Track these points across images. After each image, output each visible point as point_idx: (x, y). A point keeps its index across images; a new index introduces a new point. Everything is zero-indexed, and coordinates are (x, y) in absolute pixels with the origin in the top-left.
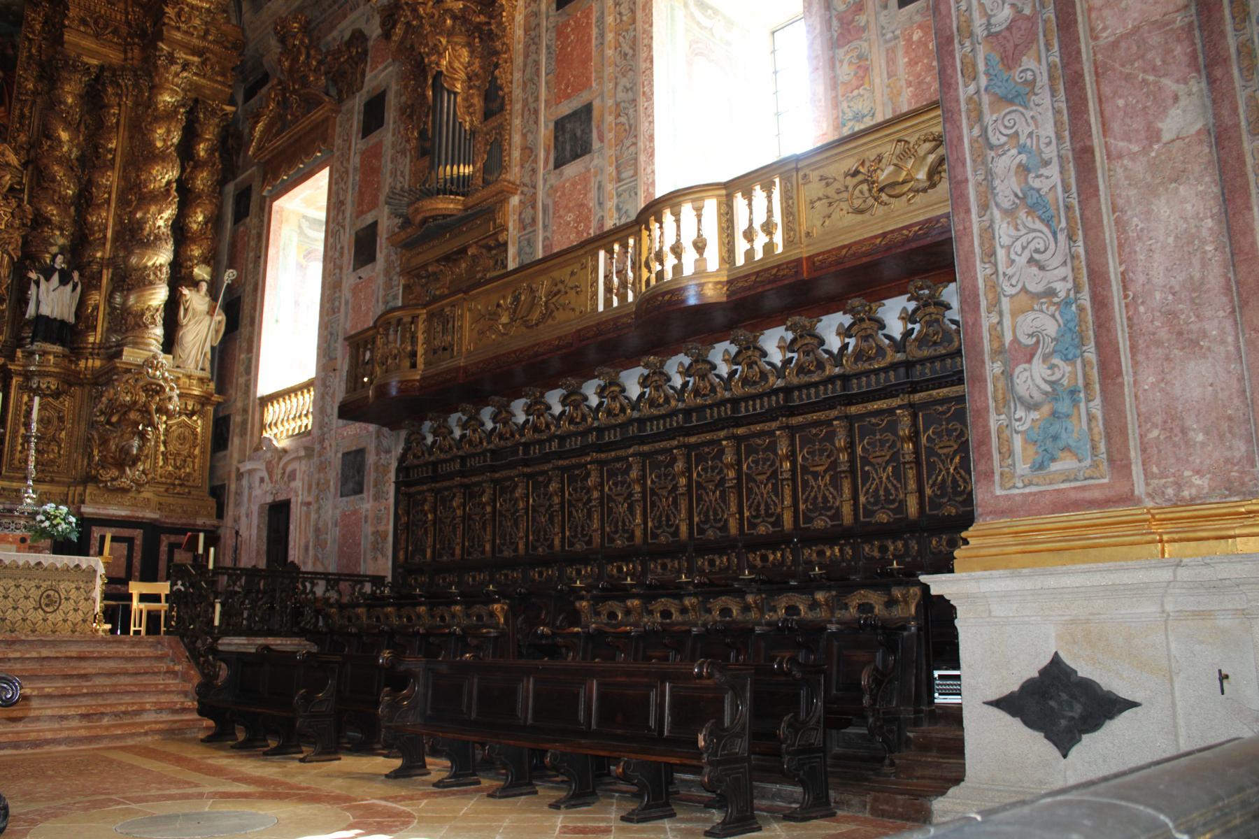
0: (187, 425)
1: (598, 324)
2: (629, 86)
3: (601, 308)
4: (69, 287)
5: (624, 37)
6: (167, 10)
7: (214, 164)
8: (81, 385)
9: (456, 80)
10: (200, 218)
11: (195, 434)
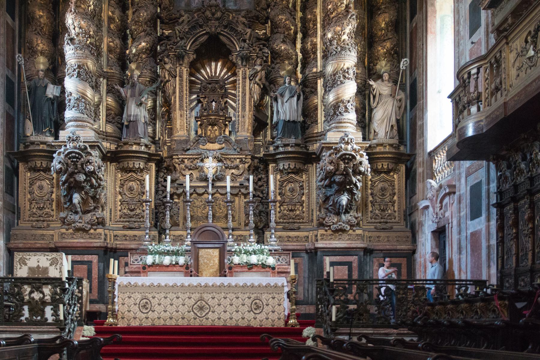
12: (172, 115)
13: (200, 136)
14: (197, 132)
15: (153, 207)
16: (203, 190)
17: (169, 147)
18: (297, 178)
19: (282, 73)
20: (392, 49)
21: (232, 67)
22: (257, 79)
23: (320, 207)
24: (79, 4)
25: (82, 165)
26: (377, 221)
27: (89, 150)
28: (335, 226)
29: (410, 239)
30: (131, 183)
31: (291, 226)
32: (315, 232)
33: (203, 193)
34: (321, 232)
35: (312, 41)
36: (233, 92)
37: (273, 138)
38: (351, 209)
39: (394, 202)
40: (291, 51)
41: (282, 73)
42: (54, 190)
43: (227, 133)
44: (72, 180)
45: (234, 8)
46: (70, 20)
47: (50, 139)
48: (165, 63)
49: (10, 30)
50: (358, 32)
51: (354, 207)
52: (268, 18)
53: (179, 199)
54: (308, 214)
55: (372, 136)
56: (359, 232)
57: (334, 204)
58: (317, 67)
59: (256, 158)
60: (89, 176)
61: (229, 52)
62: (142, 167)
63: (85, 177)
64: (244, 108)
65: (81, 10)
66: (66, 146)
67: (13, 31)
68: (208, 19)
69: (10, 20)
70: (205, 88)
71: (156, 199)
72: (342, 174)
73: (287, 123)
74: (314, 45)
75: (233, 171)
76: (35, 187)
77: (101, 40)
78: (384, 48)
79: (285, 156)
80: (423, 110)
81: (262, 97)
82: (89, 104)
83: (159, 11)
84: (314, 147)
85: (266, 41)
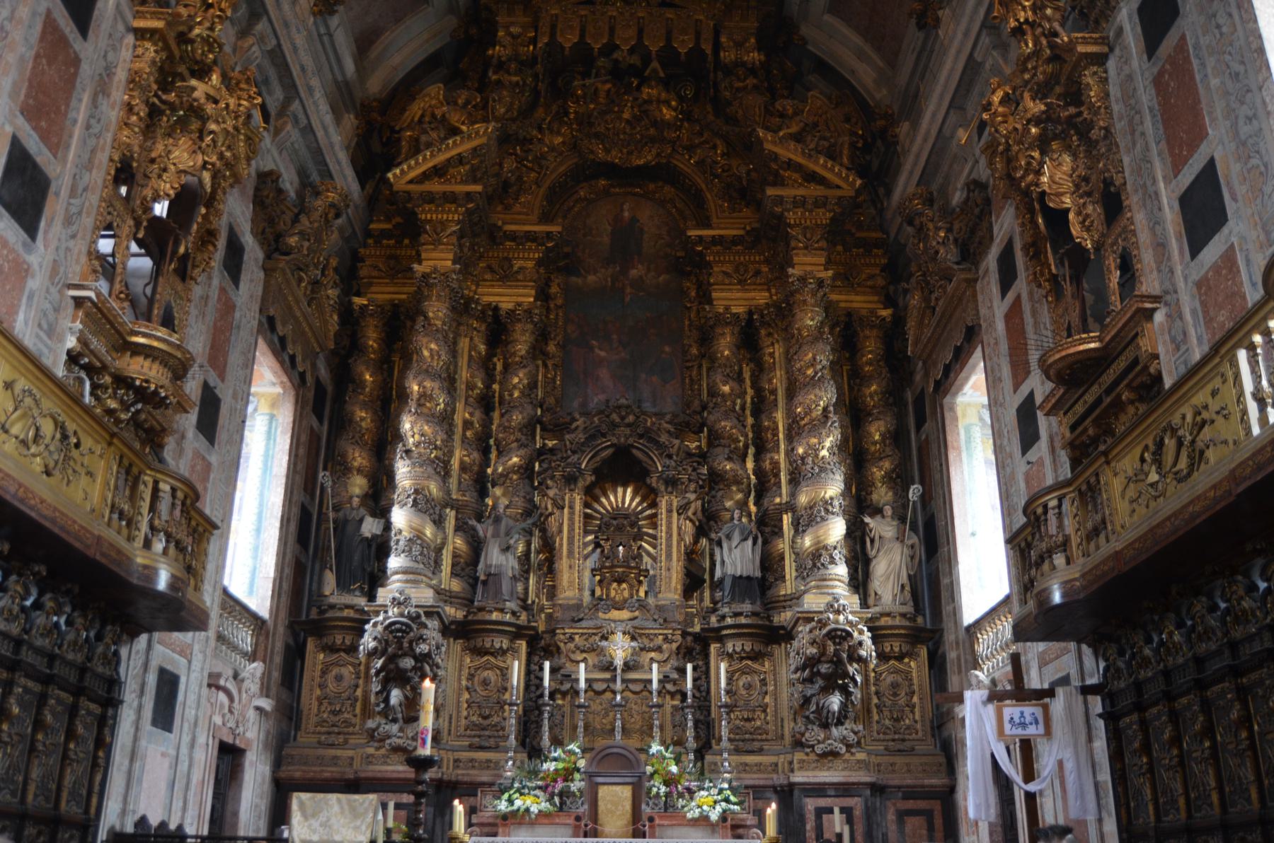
0: (897, 671)
1: (1254, 455)
2: (1250, 113)
3: (1256, 430)
5: (1230, 54)
9: (1063, 194)
12: (556, 565)
13: (600, 599)
14: (593, 593)
15: (521, 712)
16: (605, 686)
17: (550, 616)
18: (756, 666)
19: (728, 504)
20: (893, 470)
21: (650, 496)
22: (690, 513)
23: (795, 713)
24: (422, 401)
25: (411, 643)
26: (887, 737)
27: (423, 619)
28: (821, 746)
29: (944, 768)
30: (486, 673)
31: (748, 746)
32: (789, 757)
33: (605, 691)
34: (799, 756)
35: (772, 459)
36: (650, 531)
37: (714, 602)
38: (846, 717)
39: (914, 706)
40: (740, 472)
41: (728, 504)
42: (361, 682)
43: (642, 594)
44: (392, 666)
45: (654, 410)
46: (406, 425)
47: (361, 601)
48: (548, 488)
49: (314, 437)
50: (842, 447)
51: (851, 715)
52: (703, 425)
53: (563, 698)
54: (776, 725)
55: (871, 601)
56: (861, 756)
57: (819, 710)
58: (780, 495)
59: (690, 634)
60: (421, 662)
61: (645, 473)
62: (505, 647)
63: (413, 663)
64: (669, 556)
65: (425, 410)
66: (386, 612)
67: (319, 439)
68: (614, 425)
69: (315, 423)
70: (608, 525)
71: (525, 700)
72: (831, 661)
73: (737, 580)
74: (776, 465)
75: (653, 654)
76: (330, 677)
77: (451, 453)
78: (881, 469)
79: (732, 631)
80: (951, 560)
81: (696, 541)
82: (428, 547)
83: (539, 412)
84: (784, 617)
85: (703, 456)
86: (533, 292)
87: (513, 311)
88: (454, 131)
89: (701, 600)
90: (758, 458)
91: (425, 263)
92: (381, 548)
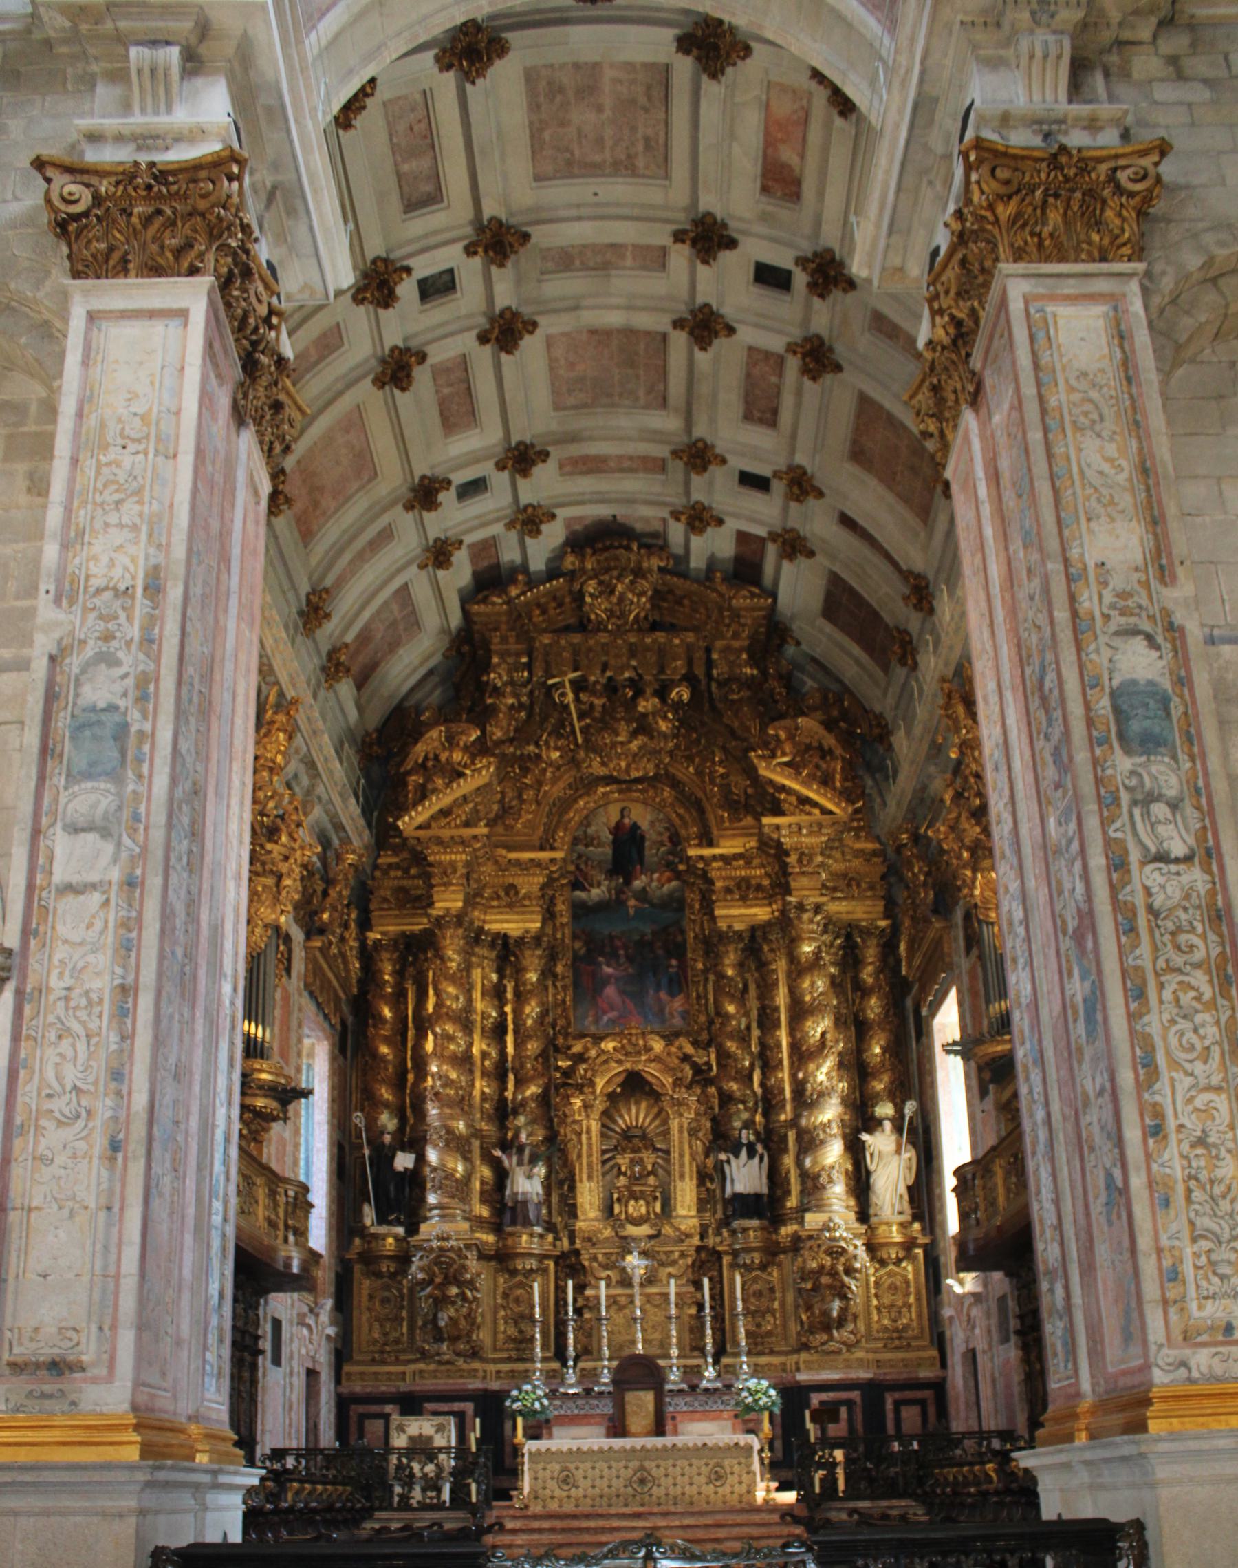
4: (756, 1160)
6: (788, 860)
7: (880, 988)
8: (784, 1252)
10: (877, 1050)
11: (907, 1282)
39: (910, 1306)
75: (670, 1270)
77: (473, 1086)
86: (539, 917)
87: (522, 938)
88: (461, 775)
89: (715, 1212)
90: (763, 1074)
91: (437, 905)
92: (415, 1180)
